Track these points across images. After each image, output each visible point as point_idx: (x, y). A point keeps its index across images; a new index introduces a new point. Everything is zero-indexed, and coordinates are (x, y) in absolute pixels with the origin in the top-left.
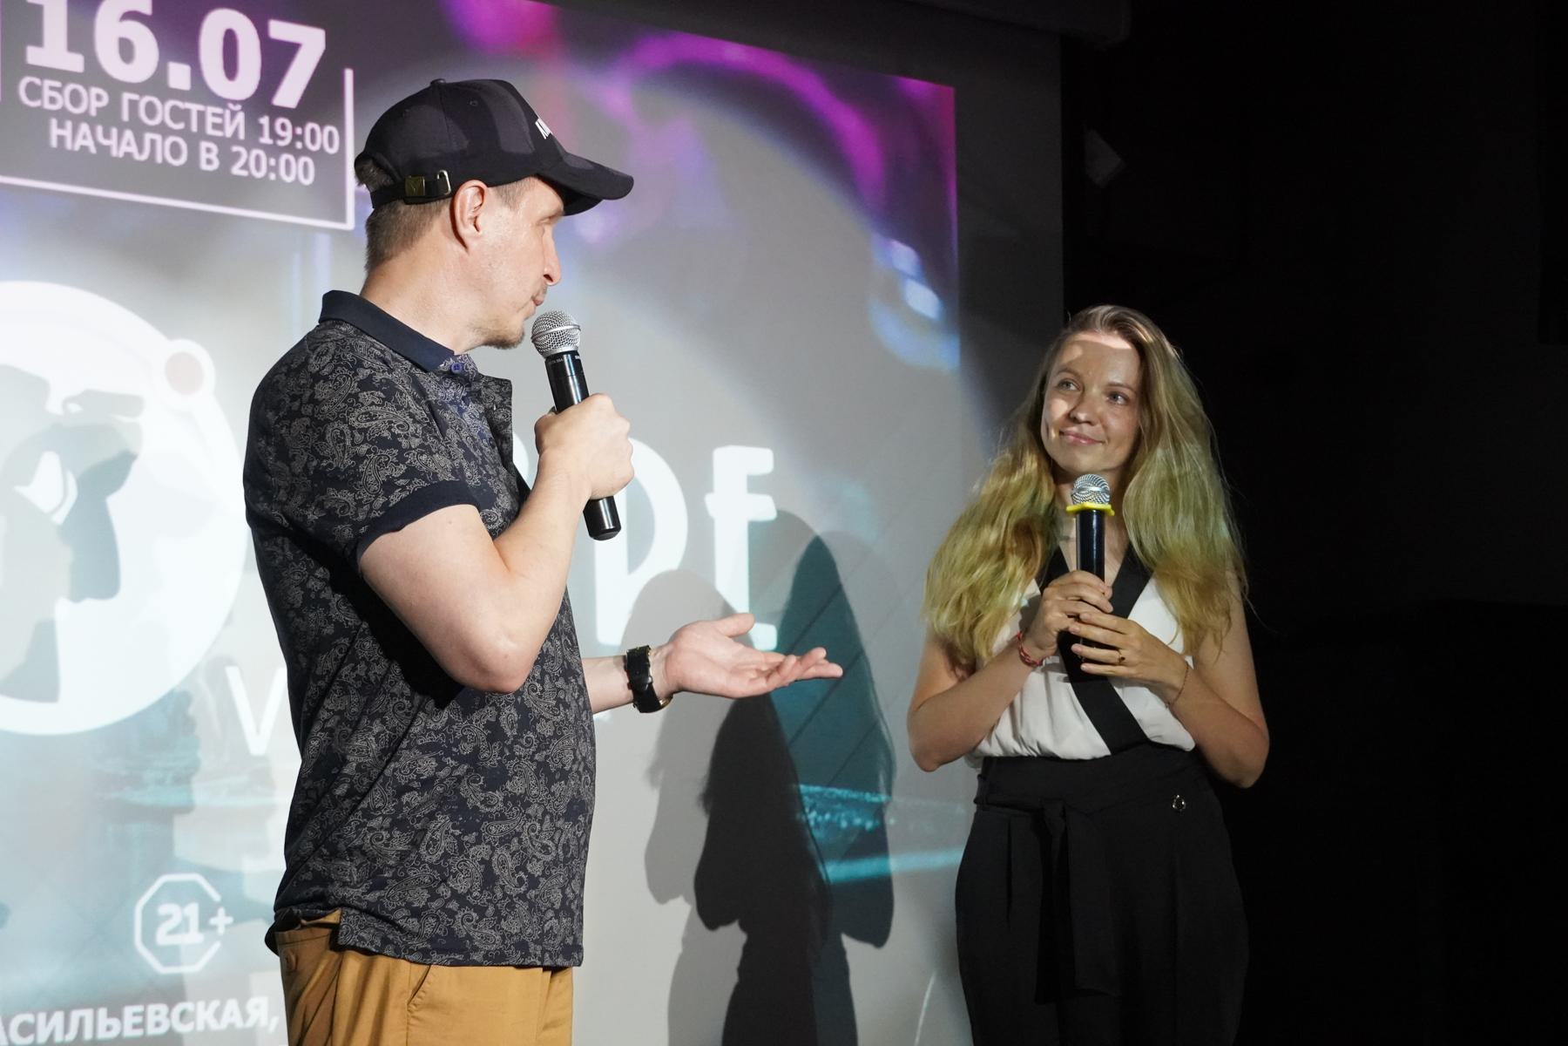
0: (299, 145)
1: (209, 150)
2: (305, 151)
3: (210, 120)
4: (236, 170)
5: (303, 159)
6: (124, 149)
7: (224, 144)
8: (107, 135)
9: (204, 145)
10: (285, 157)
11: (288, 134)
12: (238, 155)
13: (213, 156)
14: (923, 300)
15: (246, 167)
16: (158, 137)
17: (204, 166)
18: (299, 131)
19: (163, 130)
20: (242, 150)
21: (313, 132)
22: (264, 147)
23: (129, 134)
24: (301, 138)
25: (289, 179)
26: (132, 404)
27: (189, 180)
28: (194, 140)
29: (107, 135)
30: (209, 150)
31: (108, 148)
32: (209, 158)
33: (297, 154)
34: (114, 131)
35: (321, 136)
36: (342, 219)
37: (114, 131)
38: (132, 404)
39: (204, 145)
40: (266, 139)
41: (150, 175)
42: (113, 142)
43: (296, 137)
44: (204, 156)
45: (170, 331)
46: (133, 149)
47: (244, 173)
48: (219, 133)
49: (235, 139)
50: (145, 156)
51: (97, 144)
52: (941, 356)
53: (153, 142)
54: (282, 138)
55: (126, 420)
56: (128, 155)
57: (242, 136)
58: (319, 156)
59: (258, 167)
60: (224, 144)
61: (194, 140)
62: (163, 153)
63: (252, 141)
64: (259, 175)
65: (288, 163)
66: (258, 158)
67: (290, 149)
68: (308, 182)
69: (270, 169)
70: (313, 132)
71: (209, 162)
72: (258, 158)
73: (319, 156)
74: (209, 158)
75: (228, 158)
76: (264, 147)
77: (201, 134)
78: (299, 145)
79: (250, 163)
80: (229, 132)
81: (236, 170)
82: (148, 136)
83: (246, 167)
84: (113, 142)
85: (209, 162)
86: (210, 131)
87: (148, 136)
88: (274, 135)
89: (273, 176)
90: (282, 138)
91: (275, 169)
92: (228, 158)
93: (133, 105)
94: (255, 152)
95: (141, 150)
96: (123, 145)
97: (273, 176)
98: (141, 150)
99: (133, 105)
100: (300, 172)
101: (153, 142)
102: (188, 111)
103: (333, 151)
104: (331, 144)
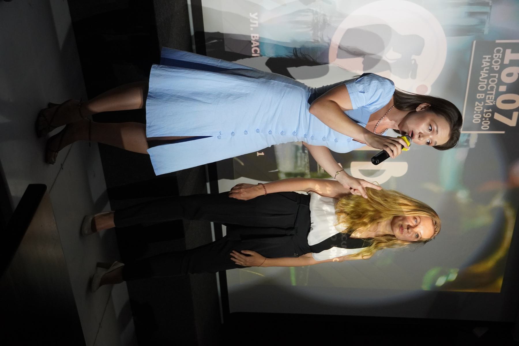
0: (484, 119)
1: (482, 96)
2: (482, 121)
4: (477, 103)
5: (480, 120)
6: (483, 74)
7: (484, 100)
8: (486, 70)
9: (484, 95)
10: (480, 115)
11: (487, 116)
12: (481, 103)
13: (481, 97)
14: (441, 282)
15: (478, 105)
16: (486, 83)
17: (478, 95)
18: (488, 119)
19: (488, 84)
20: (482, 105)
21: (487, 123)
22: (483, 110)
23: (487, 75)
24: (486, 120)
25: (474, 117)
26: (414, 76)
27: (474, 90)
28: (485, 92)
29: (486, 70)
30: (482, 96)
31: (483, 70)
32: (480, 96)
33: (481, 119)
34: (487, 72)
35: (486, 125)
36: (463, 130)
37: (487, 72)
38: (414, 76)
39: (484, 95)
40: (485, 111)
41: (475, 82)
42: (484, 71)
43: (486, 118)
44: (481, 95)
45: (433, 86)
46: (483, 77)
47: (476, 105)
48: (487, 98)
49: (485, 103)
50: (481, 79)
51: (484, 67)
52: (426, 287)
53: (484, 82)
55: (410, 75)
56: (481, 75)
57: (486, 104)
58: (481, 125)
59: (477, 109)
60: (484, 100)
61: (485, 92)
62: (481, 84)
63: (485, 107)
64: (475, 109)
65: (479, 116)
66: (480, 109)
67: (483, 117)
68: (474, 121)
69: (477, 112)
70: (487, 123)
71: (479, 96)
72: (480, 109)
73: (481, 125)
74: (480, 96)
75: (480, 101)
76: (483, 110)
77: (486, 94)
78: (484, 119)
79: (479, 107)
80: (487, 101)
81: (477, 103)
82: (486, 80)
83: (478, 105)
84: (484, 71)
85: (479, 96)
86: (487, 96)
87: (486, 80)
89: (475, 112)
91: (477, 113)
92: (480, 101)
94: (482, 108)
95: (482, 78)
96: (484, 74)
97: (475, 112)
98: (482, 78)
100: (476, 119)
101: (484, 82)
103: (482, 128)
104: (484, 127)
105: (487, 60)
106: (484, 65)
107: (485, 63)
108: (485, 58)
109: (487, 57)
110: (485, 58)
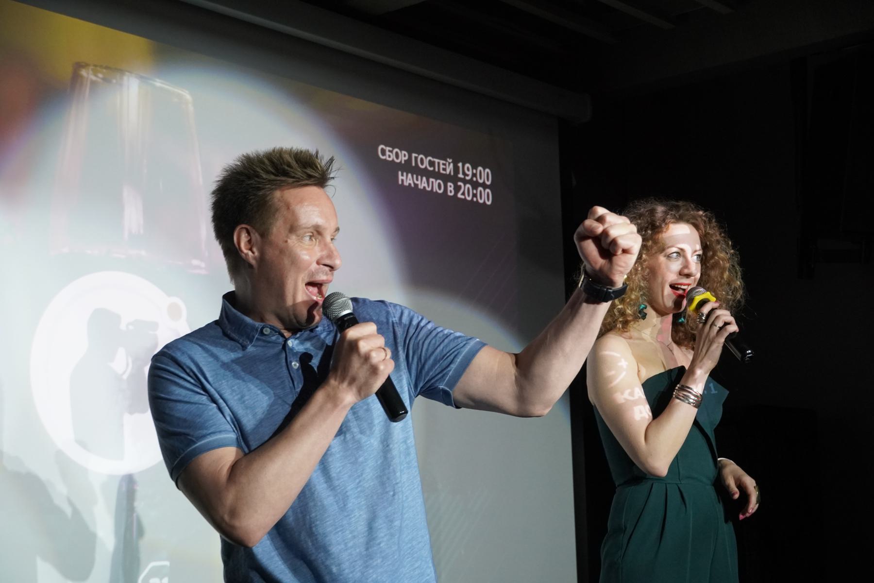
3: (442, 166)
4: (460, 195)
6: (423, 185)
11: (470, 173)
15: (463, 194)
17: (449, 194)
46: (426, 185)
47: (463, 197)
54: (468, 175)
81: (460, 195)
83: (463, 194)
84: (419, 182)
88: (464, 174)
90: (468, 175)
91: (475, 195)
93: (416, 158)
99: (416, 158)
102: (434, 162)
105: (404, 178)
106: (411, 182)
107: (409, 182)
108: (402, 180)
109: (400, 177)
110: (402, 180)
